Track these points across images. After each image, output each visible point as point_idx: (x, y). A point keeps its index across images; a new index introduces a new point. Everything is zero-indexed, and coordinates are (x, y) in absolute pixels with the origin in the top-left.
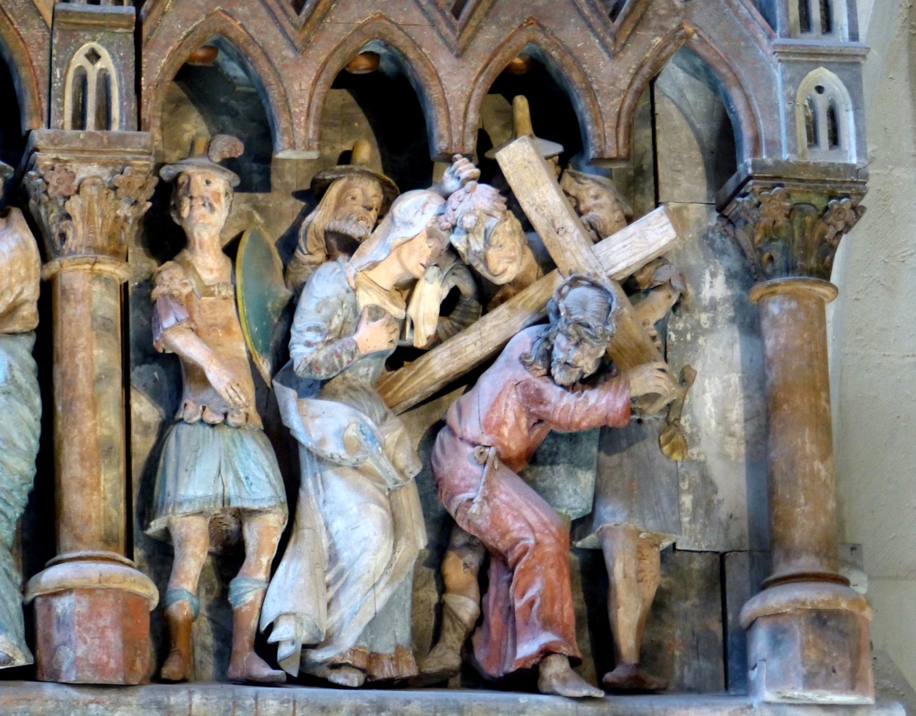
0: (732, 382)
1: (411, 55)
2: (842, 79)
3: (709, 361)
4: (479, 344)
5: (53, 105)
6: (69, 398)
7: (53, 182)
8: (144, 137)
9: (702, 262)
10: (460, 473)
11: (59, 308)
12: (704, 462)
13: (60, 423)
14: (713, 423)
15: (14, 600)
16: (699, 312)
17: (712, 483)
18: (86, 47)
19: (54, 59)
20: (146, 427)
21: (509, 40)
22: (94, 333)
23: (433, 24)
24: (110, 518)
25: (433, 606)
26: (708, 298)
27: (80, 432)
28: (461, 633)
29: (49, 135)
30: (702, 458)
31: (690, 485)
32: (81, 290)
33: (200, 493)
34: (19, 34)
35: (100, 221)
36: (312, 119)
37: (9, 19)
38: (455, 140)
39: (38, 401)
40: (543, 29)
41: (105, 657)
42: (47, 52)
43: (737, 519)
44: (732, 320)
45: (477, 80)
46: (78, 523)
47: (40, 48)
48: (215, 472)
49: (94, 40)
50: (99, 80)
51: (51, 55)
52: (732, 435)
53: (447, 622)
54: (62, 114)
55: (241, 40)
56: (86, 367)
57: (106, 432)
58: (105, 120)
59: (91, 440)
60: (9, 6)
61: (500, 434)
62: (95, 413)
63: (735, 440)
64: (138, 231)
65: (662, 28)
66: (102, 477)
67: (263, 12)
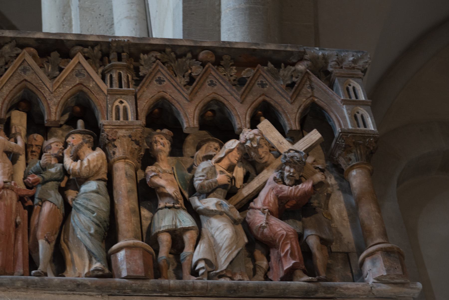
1: (226, 103)
4: (258, 182)
7: (110, 134)
8: (138, 122)
10: (257, 218)
11: (114, 173)
14: (338, 217)
17: (340, 233)
18: (119, 100)
20: (147, 219)
25: (251, 269)
28: (263, 271)
30: (336, 226)
33: (167, 224)
34: (96, 97)
39: (108, 197)
41: (137, 268)
44: (339, 190)
48: (172, 219)
49: (121, 97)
51: (107, 102)
52: (344, 220)
53: (258, 269)
54: (112, 117)
57: (133, 206)
58: (126, 117)
61: (269, 206)
67: (176, 91)
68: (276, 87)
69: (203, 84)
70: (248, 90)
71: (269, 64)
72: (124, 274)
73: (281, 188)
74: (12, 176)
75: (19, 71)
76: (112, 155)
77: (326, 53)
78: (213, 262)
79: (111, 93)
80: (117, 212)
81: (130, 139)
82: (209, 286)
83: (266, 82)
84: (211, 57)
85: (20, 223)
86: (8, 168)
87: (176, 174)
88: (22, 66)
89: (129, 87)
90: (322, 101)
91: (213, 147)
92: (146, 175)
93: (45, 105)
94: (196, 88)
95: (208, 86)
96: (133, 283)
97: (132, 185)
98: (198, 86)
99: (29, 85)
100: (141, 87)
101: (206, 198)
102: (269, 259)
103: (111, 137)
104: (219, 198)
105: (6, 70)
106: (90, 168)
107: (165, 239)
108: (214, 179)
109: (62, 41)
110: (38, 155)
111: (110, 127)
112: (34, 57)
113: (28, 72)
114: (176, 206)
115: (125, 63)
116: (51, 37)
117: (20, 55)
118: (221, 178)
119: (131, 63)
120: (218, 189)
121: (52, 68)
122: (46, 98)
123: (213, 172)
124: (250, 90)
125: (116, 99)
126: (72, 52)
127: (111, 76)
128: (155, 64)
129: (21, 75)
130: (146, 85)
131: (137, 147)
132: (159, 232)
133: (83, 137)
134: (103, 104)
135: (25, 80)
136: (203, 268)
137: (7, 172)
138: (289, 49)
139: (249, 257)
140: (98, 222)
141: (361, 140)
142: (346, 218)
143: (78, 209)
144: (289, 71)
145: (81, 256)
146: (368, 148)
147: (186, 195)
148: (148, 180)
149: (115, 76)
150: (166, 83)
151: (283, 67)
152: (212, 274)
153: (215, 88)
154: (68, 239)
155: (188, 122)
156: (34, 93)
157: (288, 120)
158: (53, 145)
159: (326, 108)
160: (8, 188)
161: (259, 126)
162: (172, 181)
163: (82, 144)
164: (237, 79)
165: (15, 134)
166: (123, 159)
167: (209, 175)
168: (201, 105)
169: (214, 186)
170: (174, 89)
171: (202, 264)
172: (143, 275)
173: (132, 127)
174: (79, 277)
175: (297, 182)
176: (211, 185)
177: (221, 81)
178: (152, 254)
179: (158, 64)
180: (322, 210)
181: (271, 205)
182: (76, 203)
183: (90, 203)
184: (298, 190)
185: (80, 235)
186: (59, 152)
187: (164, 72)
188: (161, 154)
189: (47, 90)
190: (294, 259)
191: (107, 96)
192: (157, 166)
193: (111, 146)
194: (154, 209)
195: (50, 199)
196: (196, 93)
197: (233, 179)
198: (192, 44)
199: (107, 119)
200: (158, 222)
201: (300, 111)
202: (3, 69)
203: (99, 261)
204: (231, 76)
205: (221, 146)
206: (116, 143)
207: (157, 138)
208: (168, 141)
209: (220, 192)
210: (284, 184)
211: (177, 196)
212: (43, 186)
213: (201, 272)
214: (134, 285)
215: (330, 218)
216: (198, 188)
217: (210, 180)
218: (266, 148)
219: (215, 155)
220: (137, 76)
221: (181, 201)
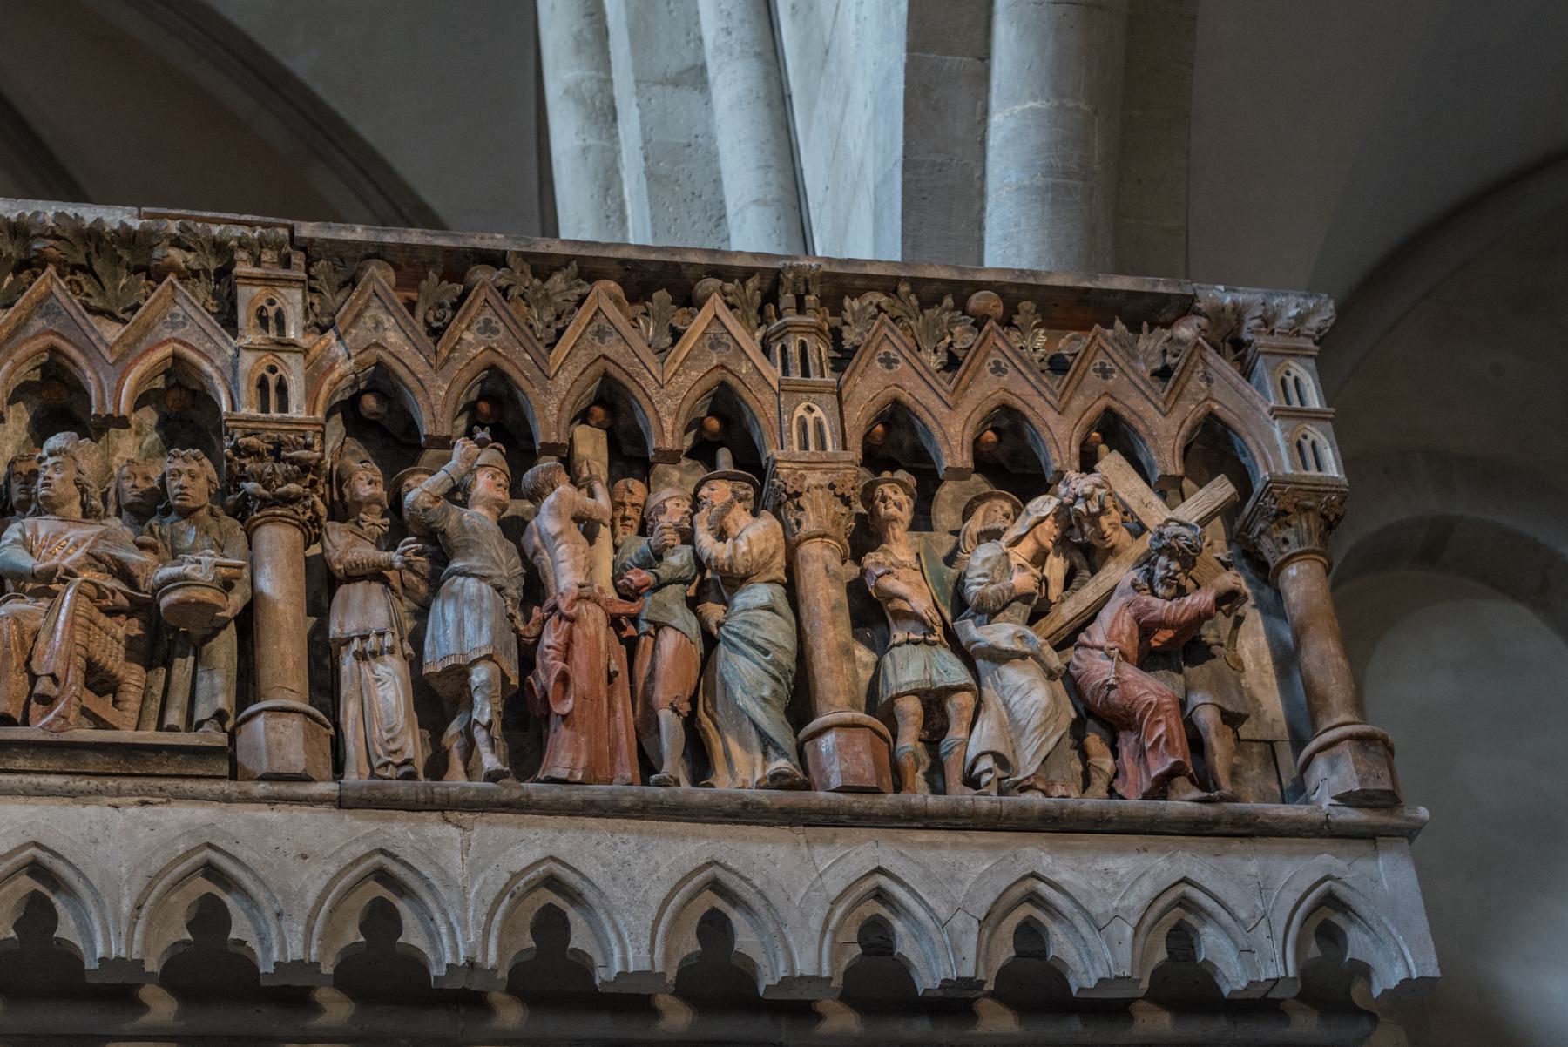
1: (1028, 412)
18: (804, 405)
20: (866, 665)
23: (1041, 395)
39: (793, 620)
40: (1115, 399)
46: (830, 696)
47: (772, 406)
54: (791, 443)
56: (825, 599)
59: (834, 644)
67: (924, 385)
68: (1133, 376)
69: (978, 369)
70: (1074, 383)
71: (1118, 322)
72: (836, 782)
73: (1147, 604)
74: (590, 568)
75: (589, 336)
76: (795, 527)
77: (1241, 298)
79: (786, 388)
80: (812, 651)
84: (996, 306)
85: (616, 673)
86: (583, 556)
87: (926, 572)
88: (595, 324)
89: (823, 376)
92: (864, 572)
93: (650, 413)
94: (966, 378)
97: (837, 594)
98: (969, 374)
99: (612, 369)
100: (850, 375)
101: (988, 623)
102: (1115, 753)
104: (1016, 623)
105: (560, 333)
107: (911, 708)
108: (1006, 582)
109: (677, 265)
110: (636, 526)
111: (789, 465)
112: (617, 302)
113: (607, 339)
115: (813, 320)
116: (653, 257)
117: (590, 298)
118: (1022, 580)
119: (824, 320)
121: (656, 329)
122: (650, 399)
123: (1004, 564)
124: (1078, 384)
125: (799, 403)
126: (700, 291)
127: (784, 349)
128: (877, 323)
129: (593, 345)
130: (859, 370)
132: (898, 696)
135: (605, 357)
137: (582, 563)
138: (1161, 289)
140: (776, 673)
143: (733, 645)
144: (1158, 341)
145: (744, 745)
147: (948, 617)
148: (871, 584)
149: (794, 349)
150: (902, 365)
151: (1145, 332)
153: (1006, 378)
154: (714, 706)
155: (952, 455)
156: (626, 388)
157: (1158, 453)
158: (667, 504)
160: (588, 598)
161: (1099, 466)
162: (919, 586)
163: (731, 502)
164: (1047, 359)
165: (590, 479)
166: (819, 536)
167: (996, 574)
168: (976, 417)
170: (919, 380)
171: (986, 763)
173: (834, 466)
174: (743, 787)
177: (1016, 362)
178: (888, 743)
179: (883, 323)
182: (728, 631)
183: (759, 633)
184: (1183, 608)
185: (743, 700)
186: (682, 519)
187: (897, 343)
189: (653, 379)
190: (1173, 755)
191: (778, 395)
194: (881, 646)
195: (674, 623)
196: (966, 389)
197: (1044, 581)
198: (955, 276)
200: (895, 673)
202: (553, 331)
203: (784, 755)
204: (1035, 350)
206: (803, 501)
207: (887, 490)
209: (1017, 611)
210: (1154, 594)
212: (656, 595)
213: (986, 778)
214: (855, 805)
216: (975, 602)
217: (1000, 585)
218: (1115, 516)
219: (1005, 529)
220: (835, 350)
221: (939, 630)
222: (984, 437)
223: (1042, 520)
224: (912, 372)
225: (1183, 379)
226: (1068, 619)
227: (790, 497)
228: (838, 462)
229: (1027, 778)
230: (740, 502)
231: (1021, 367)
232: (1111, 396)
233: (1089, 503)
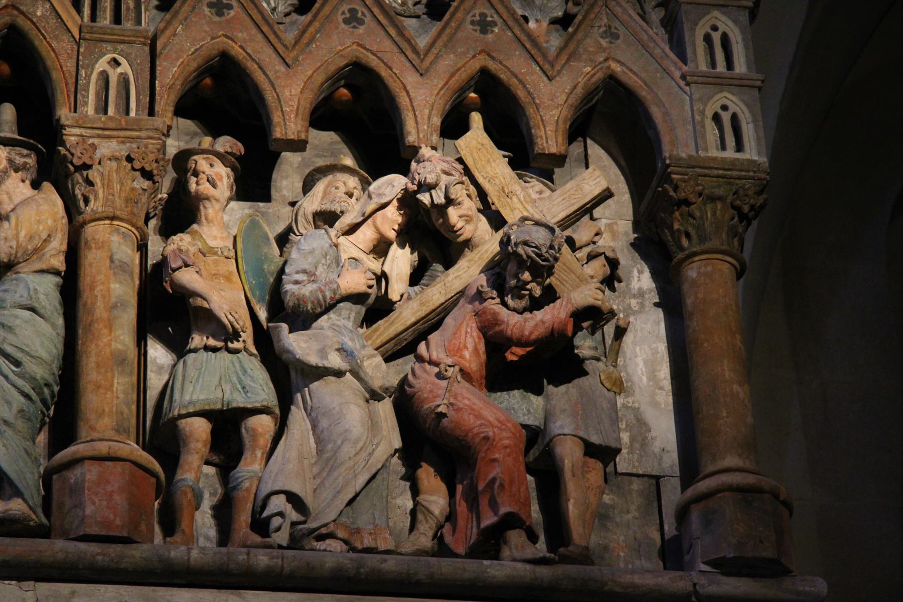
0: (659, 350)
1: (384, 73)
2: (742, 100)
3: (639, 334)
4: (443, 292)
5: (79, 96)
6: (89, 321)
7: (77, 153)
9: (630, 262)
11: (82, 255)
12: (639, 408)
13: (80, 342)
14: (645, 379)
15: (32, 473)
16: (629, 298)
17: (645, 424)
18: (109, 57)
19: (81, 63)
20: (160, 368)
21: (463, 66)
22: (112, 271)
24: (122, 413)
25: (408, 511)
26: (636, 288)
27: (97, 345)
28: (433, 523)
29: (74, 117)
30: (636, 405)
31: (627, 425)
32: (101, 240)
34: (51, 46)
35: (119, 187)
36: (300, 116)
37: (43, 35)
38: (421, 136)
39: (60, 321)
40: (493, 58)
42: (75, 61)
43: (668, 452)
45: (438, 93)
46: (92, 417)
50: (119, 82)
52: (661, 388)
53: (420, 516)
54: (86, 104)
55: (241, 57)
56: (104, 297)
57: (120, 347)
60: (43, 24)
61: (462, 357)
62: (111, 332)
63: (664, 393)
64: (156, 224)
65: (591, 61)
66: (116, 381)
67: (260, 37)
76: (82, 204)
78: (309, 500)
81: (129, 165)
82: (285, 565)
83: (495, 16)
87: (240, 260)
90: (634, 73)
91: (343, 189)
94: (312, 29)
95: (343, 26)
96: (98, 554)
98: (317, 24)
103: (80, 158)
106: (18, 242)
114: (230, 345)
120: (341, 304)
130: (181, 16)
131: (146, 184)
133: (9, 153)
134: (67, 66)
136: (281, 514)
139: (404, 478)
140: (27, 389)
141: (719, 187)
142: (667, 384)
146: (738, 209)
147: (262, 315)
152: (301, 530)
153: (361, 30)
159: (643, 93)
166: (107, 218)
168: (320, 78)
169: (328, 300)
170: (254, 31)
171: (278, 503)
172: (125, 534)
175: (536, 304)
176: (321, 297)
180: (601, 365)
181: (467, 354)
188: (207, 203)
192: (194, 234)
193: (81, 181)
197: (382, 277)
199: (75, 111)
201: (570, 101)
205: (365, 184)
206: (93, 174)
208: (229, 169)
209: (345, 313)
211: (235, 323)
214: (100, 558)
215: (619, 386)
218: (470, 205)
221: (247, 336)
222: (337, 94)
223: (384, 206)
224: (248, 19)
225: (580, 35)
226: (409, 323)
227: (78, 169)
228: (141, 130)
229: (325, 525)
230: (16, 171)
231: (381, 18)
232: (489, 55)
233: (433, 192)
